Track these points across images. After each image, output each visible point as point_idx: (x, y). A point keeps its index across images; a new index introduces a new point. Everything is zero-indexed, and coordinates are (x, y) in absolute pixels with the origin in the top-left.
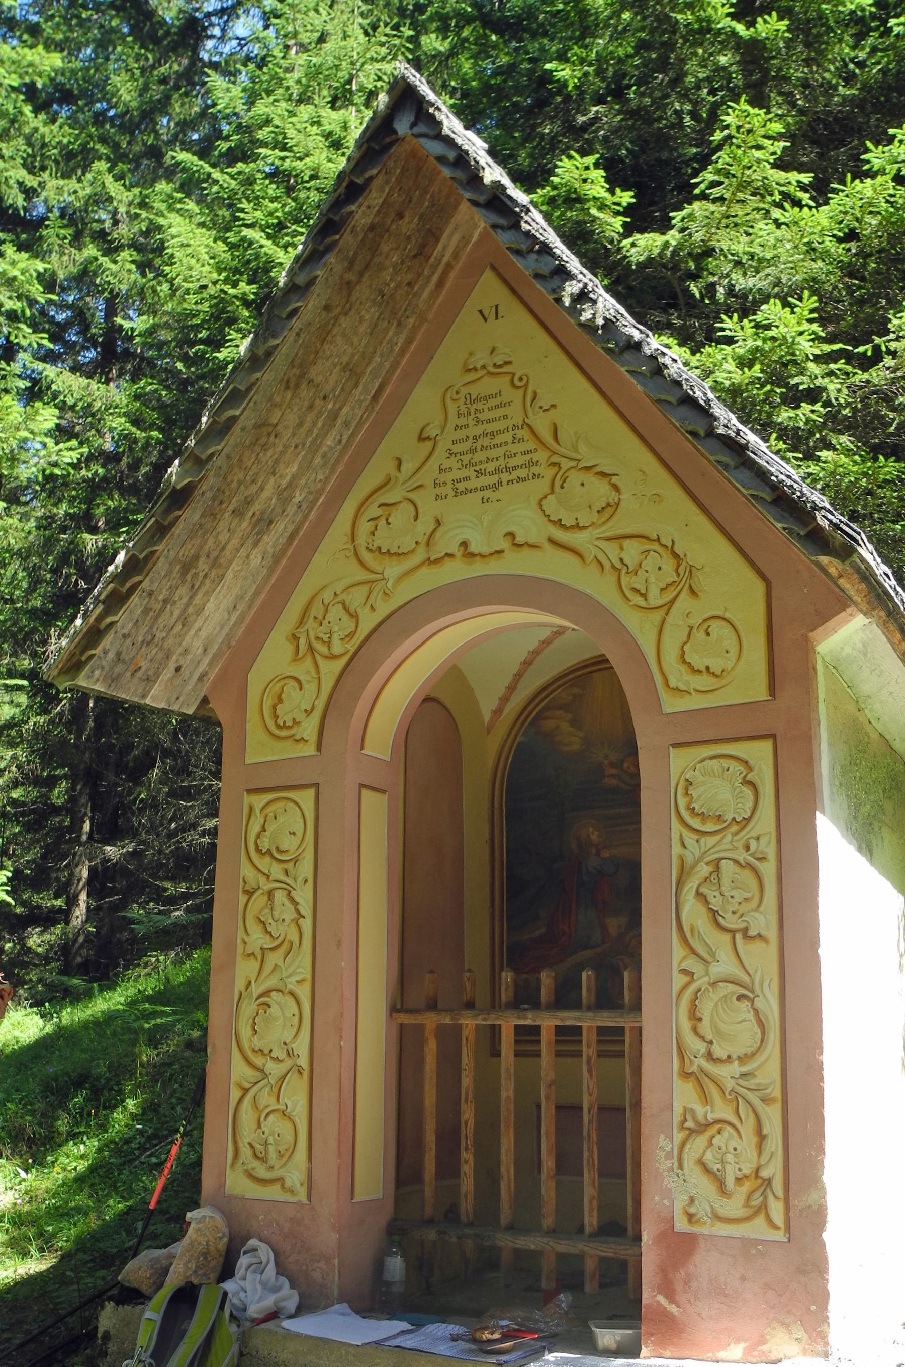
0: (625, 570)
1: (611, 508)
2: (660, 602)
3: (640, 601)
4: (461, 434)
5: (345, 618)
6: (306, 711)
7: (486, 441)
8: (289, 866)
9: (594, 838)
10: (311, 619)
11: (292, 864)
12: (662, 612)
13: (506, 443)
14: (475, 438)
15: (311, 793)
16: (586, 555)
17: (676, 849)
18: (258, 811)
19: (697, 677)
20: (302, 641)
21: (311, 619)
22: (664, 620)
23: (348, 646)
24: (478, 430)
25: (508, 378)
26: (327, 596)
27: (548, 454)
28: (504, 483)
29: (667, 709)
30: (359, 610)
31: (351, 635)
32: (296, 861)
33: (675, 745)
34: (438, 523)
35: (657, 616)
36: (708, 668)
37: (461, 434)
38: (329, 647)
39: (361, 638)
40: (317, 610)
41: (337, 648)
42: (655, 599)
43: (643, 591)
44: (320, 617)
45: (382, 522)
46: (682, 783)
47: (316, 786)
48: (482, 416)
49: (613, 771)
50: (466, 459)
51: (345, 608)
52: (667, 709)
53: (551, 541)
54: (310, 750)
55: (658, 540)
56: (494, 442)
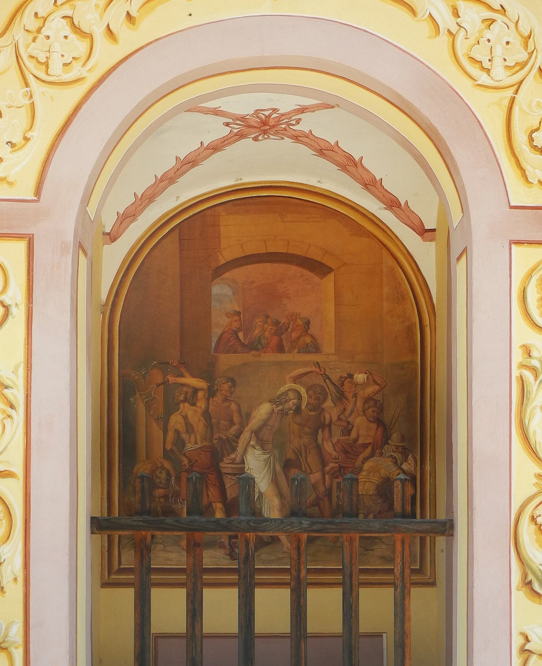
16: (418, 9)
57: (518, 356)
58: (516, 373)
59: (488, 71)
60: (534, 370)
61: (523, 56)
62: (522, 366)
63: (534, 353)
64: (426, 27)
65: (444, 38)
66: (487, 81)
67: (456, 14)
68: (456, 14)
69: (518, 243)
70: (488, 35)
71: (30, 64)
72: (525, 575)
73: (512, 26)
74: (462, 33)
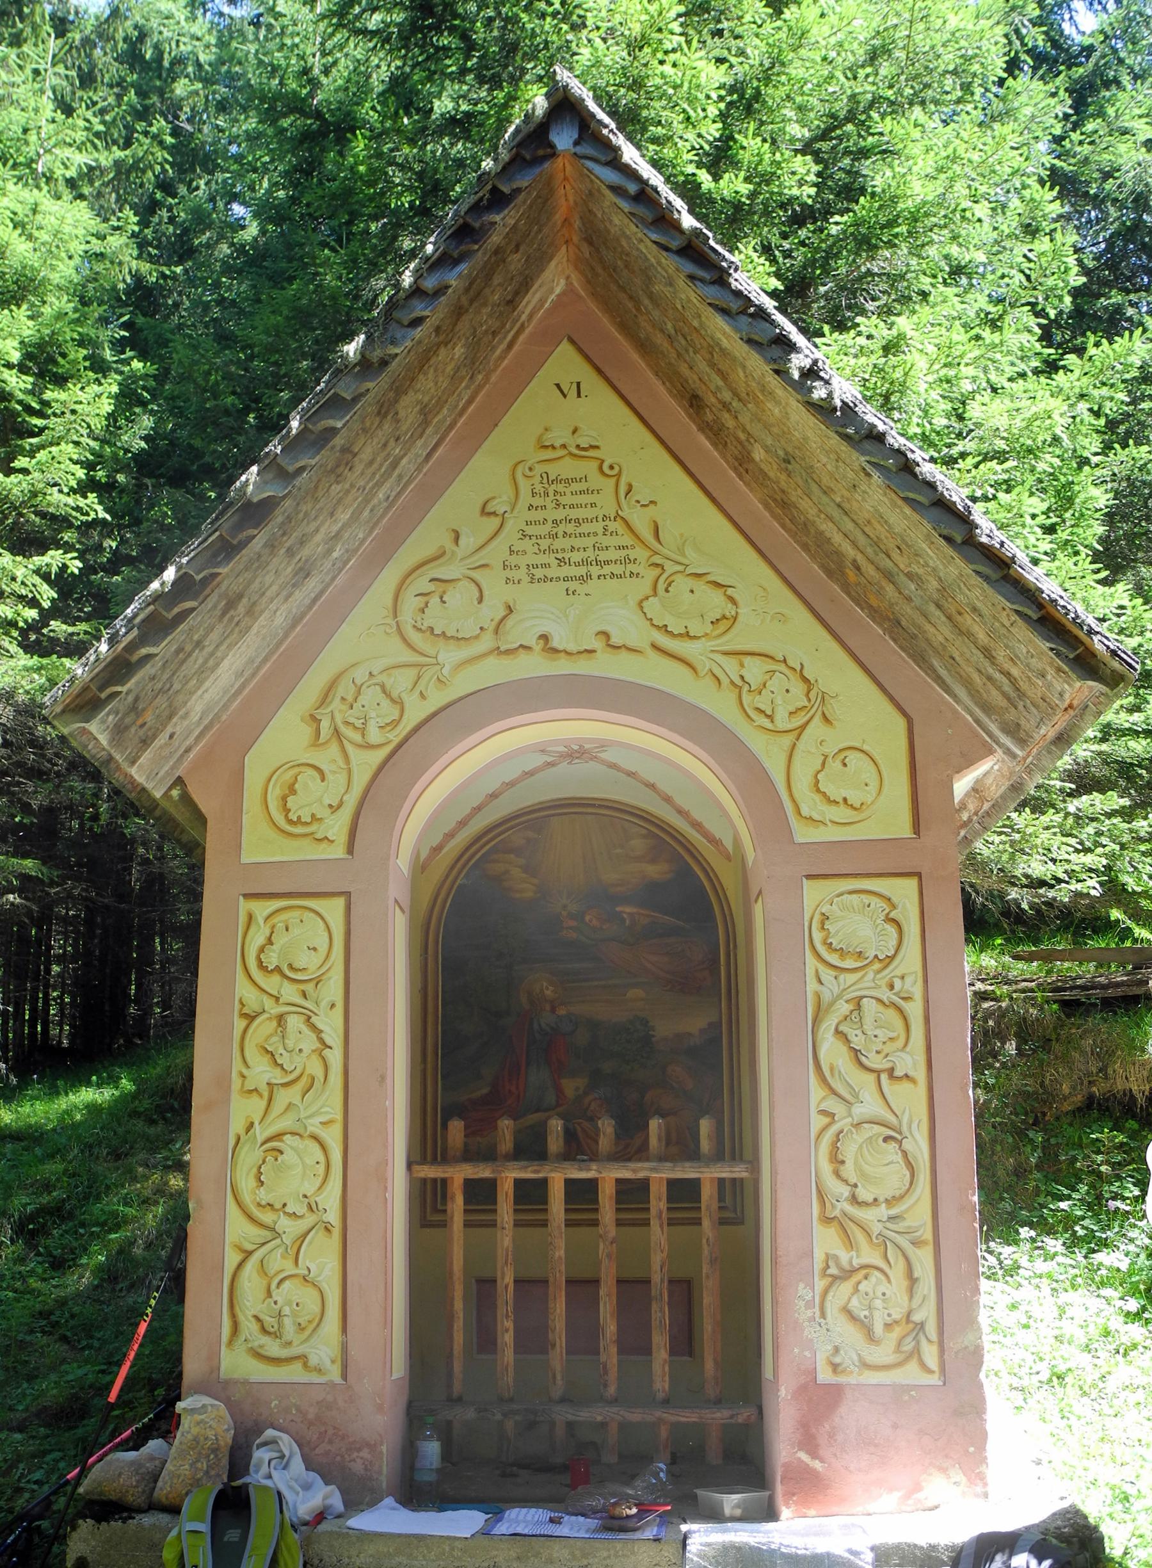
0: (746, 688)
1: (725, 622)
2: (789, 727)
3: (767, 723)
5: (385, 703)
6: (330, 806)
7: (570, 528)
8: (309, 988)
9: (548, 993)
10: (337, 700)
11: (311, 985)
12: (791, 737)
13: (595, 534)
14: (555, 522)
15: (340, 902)
16: (699, 668)
17: (812, 986)
18: (261, 921)
19: (834, 808)
20: (325, 724)
21: (337, 700)
23: (390, 736)
24: (560, 514)
25: (596, 464)
26: (360, 675)
27: (647, 553)
28: (595, 576)
29: (799, 839)
30: (404, 695)
31: (395, 723)
32: (318, 981)
33: (809, 877)
34: (510, 610)
35: (787, 740)
36: (845, 800)
38: (363, 735)
39: (408, 728)
40: (345, 689)
41: (374, 736)
43: (769, 712)
44: (350, 698)
45: (435, 600)
46: (817, 918)
47: (347, 895)
48: (566, 500)
49: (573, 923)
50: (545, 544)
51: (384, 691)
52: (799, 839)
53: (655, 646)
54: (338, 851)
55: (785, 661)
56: (579, 530)
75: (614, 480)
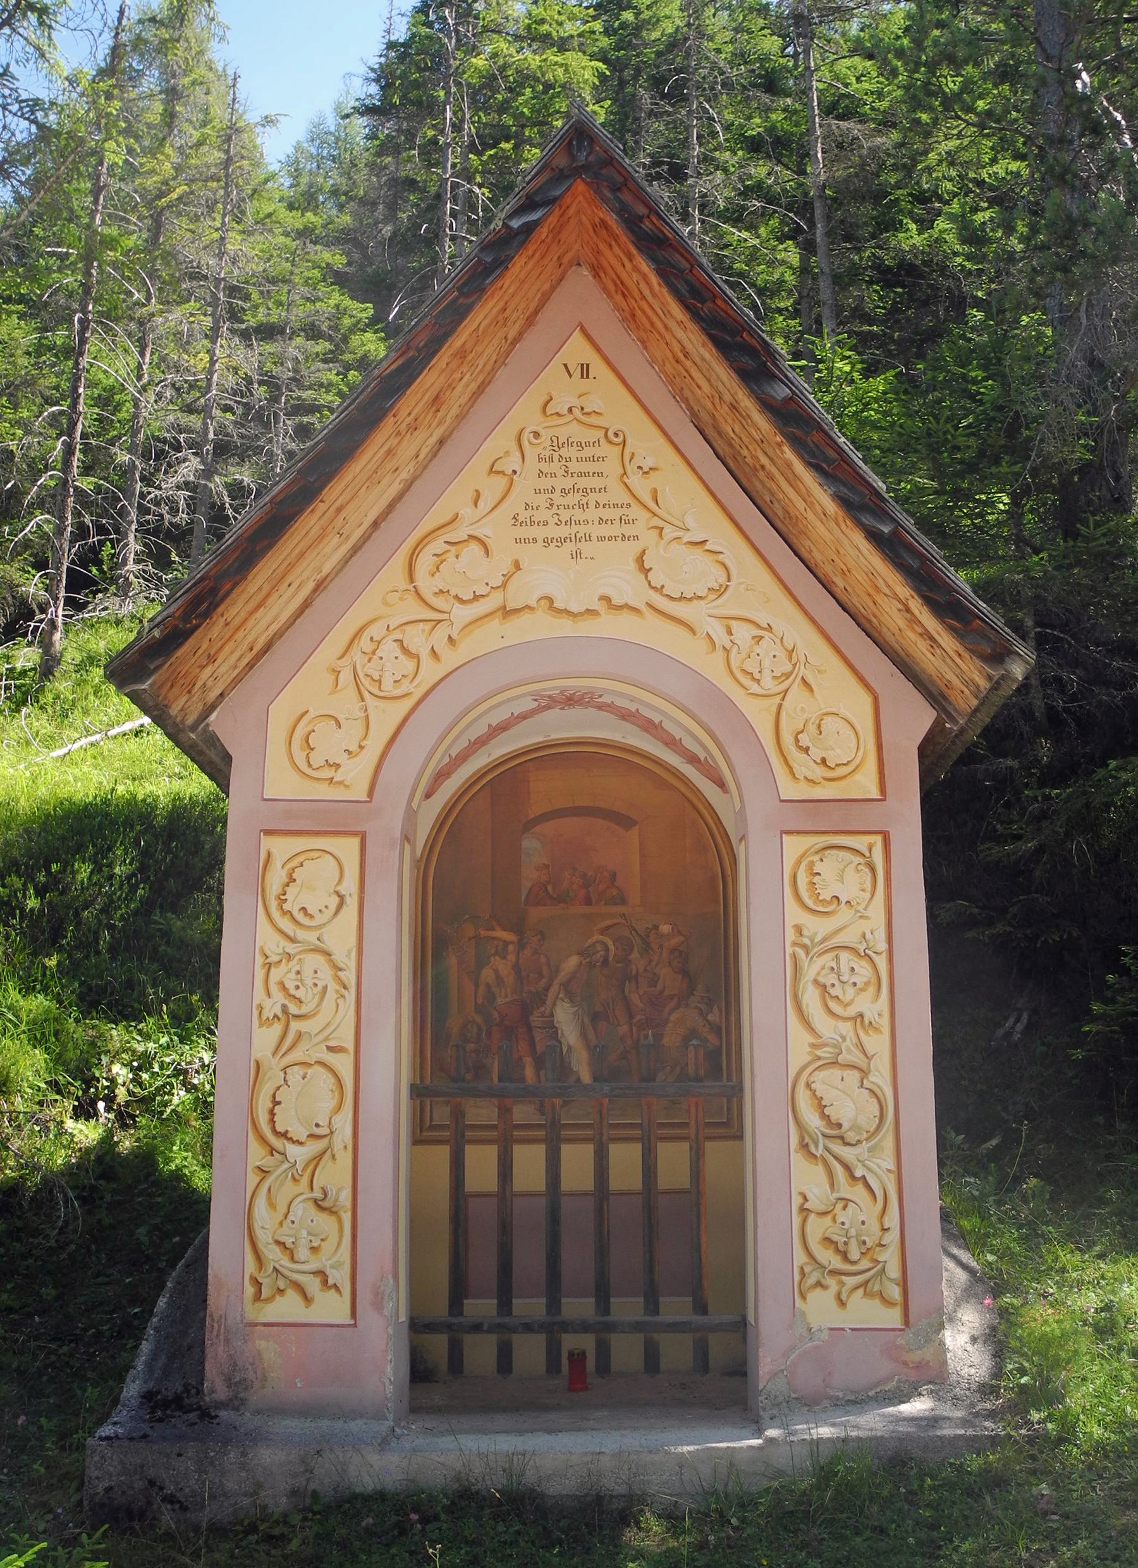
4: (547, 483)
16: (697, 629)
22: (780, 706)
24: (568, 483)
37: (547, 483)
42: (768, 683)
45: (451, 557)
57: (790, 936)
58: (789, 950)
59: (758, 681)
60: (804, 947)
61: (788, 667)
62: (795, 944)
63: (805, 932)
64: (704, 644)
65: (720, 654)
66: (759, 691)
67: (730, 633)
68: (730, 633)
69: (788, 832)
70: (757, 650)
71: (366, 682)
72: (802, 1138)
73: (778, 641)
74: (735, 649)
75: (618, 449)
